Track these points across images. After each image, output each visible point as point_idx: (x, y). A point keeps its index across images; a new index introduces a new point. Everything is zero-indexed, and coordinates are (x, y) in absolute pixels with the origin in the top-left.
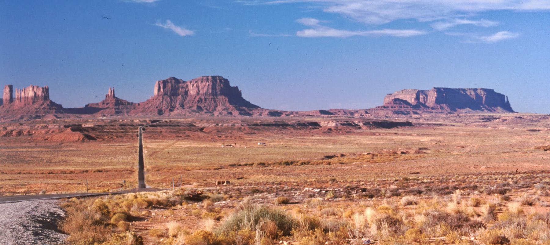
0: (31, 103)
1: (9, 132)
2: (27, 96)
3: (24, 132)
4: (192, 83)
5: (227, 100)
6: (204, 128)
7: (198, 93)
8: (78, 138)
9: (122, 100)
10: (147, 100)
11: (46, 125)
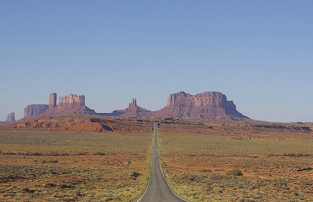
0: (70, 108)
3: (52, 125)
5: (224, 111)
6: (213, 127)
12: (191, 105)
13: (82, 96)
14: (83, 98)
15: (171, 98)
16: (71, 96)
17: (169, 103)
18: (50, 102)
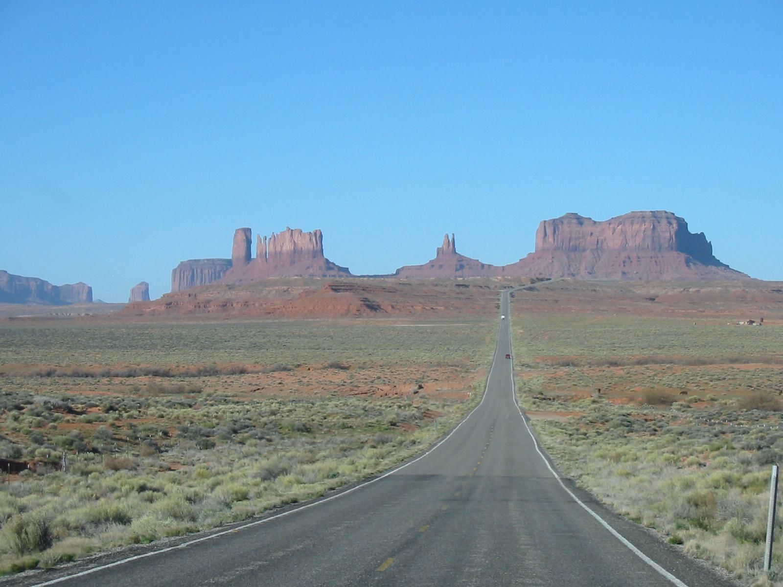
1: (202, 305)
2: (278, 249)
6: (657, 297)
7: (624, 247)
8: (346, 308)
9: (471, 260)
10: (520, 260)
11: (285, 288)
12: (595, 247)
13: (315, 234)
14: (319, 236)
16: (288, 235)
17: (540, 244)
18: (234, 250)
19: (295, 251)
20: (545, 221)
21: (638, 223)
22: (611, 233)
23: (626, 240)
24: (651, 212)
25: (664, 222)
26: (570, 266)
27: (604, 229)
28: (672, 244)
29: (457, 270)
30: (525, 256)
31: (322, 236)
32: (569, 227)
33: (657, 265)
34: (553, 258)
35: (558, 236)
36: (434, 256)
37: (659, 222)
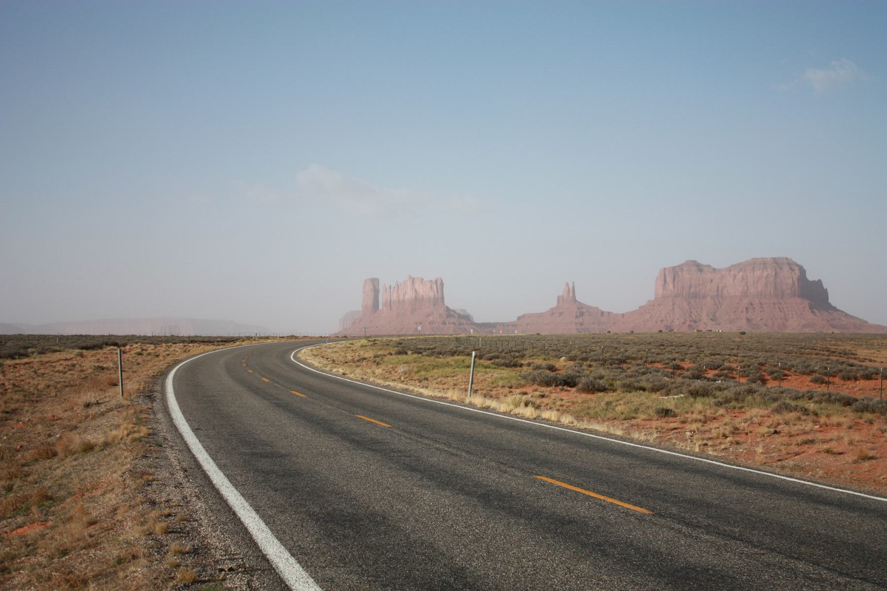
2: (401, 297)
4: (732, 273)
9: (591, 307)
10: (640, 307)
12: (715, 294)
13: (436, 282)
14: (439, 285)
15: (663, 277)
16: (409, 283)
17: (660, 292)
19: (416, 299)
20: (665, 269)
21: (760, 269)
22: (732, 280)
23: (747, 287)
24: (773, 258)
25: (786, 268)
26: (691, 313)
27: (724, 276)
28: (794, 290)
29: (577, 317)
30: (644, 303)
31: (443, 284)
32: (689, 274)
33: (781, 311)
34: (673, 304)
35: (678, 283)
36: (554, 304)
37: (781, 269)
